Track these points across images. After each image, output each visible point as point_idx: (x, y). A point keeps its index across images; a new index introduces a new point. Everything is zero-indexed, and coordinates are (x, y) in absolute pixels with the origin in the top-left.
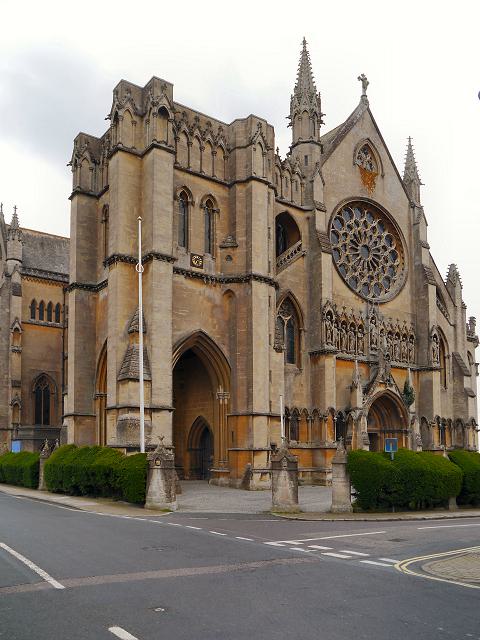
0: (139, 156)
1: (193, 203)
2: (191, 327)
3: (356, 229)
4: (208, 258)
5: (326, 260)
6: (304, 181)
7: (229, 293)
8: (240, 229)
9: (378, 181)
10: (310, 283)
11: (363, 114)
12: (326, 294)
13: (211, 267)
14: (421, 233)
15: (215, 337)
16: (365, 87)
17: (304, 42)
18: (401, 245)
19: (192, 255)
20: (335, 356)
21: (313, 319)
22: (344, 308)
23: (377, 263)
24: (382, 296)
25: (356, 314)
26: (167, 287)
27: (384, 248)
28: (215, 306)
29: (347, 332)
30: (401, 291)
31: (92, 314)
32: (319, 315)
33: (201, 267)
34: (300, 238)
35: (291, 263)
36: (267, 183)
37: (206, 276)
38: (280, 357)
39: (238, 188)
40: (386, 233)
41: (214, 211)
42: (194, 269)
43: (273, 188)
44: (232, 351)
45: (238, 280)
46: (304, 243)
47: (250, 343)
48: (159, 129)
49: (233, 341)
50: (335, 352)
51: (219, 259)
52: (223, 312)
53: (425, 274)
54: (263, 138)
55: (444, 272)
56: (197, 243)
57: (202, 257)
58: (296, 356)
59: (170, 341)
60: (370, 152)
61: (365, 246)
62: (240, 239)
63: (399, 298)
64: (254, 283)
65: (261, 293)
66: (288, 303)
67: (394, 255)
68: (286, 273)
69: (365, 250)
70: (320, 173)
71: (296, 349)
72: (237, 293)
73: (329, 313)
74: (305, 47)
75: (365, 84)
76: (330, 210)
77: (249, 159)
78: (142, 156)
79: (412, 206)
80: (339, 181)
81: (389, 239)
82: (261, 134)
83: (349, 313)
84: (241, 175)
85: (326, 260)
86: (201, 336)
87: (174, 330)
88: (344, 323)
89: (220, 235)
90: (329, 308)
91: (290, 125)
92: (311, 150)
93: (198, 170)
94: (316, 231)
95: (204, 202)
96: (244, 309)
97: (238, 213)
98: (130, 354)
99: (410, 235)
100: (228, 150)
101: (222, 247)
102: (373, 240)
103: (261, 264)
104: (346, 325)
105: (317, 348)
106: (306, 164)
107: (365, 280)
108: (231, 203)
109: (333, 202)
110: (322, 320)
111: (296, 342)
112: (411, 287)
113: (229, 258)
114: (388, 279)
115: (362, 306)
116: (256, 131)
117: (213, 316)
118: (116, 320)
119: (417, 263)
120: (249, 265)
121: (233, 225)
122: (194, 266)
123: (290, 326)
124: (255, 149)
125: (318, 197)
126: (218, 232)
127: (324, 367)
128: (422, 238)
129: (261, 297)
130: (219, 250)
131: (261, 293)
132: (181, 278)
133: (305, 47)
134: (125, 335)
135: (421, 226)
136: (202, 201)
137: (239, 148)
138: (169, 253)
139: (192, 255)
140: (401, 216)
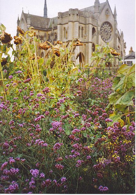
8: (87, 33)
9: (109, 17)
18: (112, 29)
34: (95, 32)
39: (87, 25)
44: (85, 55)
45: (86, 42)
46: (96, 33)
47: (88, 54)
49: (85, 53)
60: (108, 10)
67: (111, 31)
77: (89, 20)
79: (115, 20)
80: (102, 18)
84: (87, 23)
85: (100, 36)
89: (84, 34)
108: (86, 27)
109: (101, 23)
120: (88, 40)
121: (86, 32)
125: (99, 24)
131: (90, 45)
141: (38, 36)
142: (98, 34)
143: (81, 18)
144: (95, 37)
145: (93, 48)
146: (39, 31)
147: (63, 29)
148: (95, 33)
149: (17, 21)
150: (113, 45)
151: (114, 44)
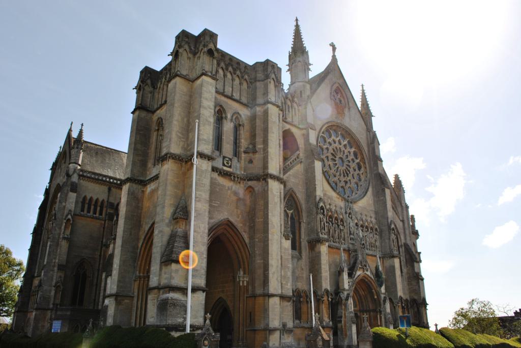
0: (188, 80)
1: (226, 118)
2: (221, 216)
3: (334, 145)
4: (235, 160)
5: (318, 165)
6: (300, 108)
7: (250, 189)
8: (259, 139)
9: (346, 111)
10: (307, 183)
11: (333, 69)
12: (319, 193)
13: (237, 168)
14: (376, 150)
15: (239, 226)
16: (334, 49)
17: (297, 20)
18: (363, 158)
19: (224, 157)
20: (327, 244)
21: (309, 213)
22: (330, 205)
23: (349, 171)
24: (354, 196)
25: (338, 209)
26: (207, 182)
27: (353, 160)
28: (239, 200)
29: (332, 224)
30: (366, 193)
31: (140, 205)
32: (315, 210)
33: (230, 167)
34: (298, 149)
35: (293, 167)
36: (278, 106)
37: (234, 174)
38: (287, 244)
40: (353, 150)
41: (240, 125)
42: (225, 168)
43: (282, 110)
44: (252, 238)
45: (257, 178)
47: (266, 231)
48: (205, 62)
49: (252, 228)
50: (327, 241)
51: (243, 162)
52: (245, 205)
53: (381, 179)
54: (275, 75)
55: (392, 180)
56: (228, 149)
57: (231, 160)
58: (297, 244)
59: (207, 226)
61: (341, 158)
62: (259, 146)
63: (365, 198)
64: (270, 181)
65: (275, 188)
66: (290, 200)
68: (289, 175)
69: (340, 161)
70: (310, 102)
71: (297, 238)
72: (256, 189)
73: (322, 208)
74: (297, 23)
75: (333, 47)
76: (318, 128)
78: (193, 81)
81: (355, 154)
82: (274, 72)
83: (333, 208)
85: (318, 165)
86: (229, 224)
87: (210, 218)
88: (331, 217)
89: (244, 143)
90: (321, 204)
91: (289, 70)
92: (304, 86)
93: (230, 95)
94: (310, 144)
95: (234, 117)
96: (262, 202)
97: (257, 128)
98: (173, 237)
99: (369, 151)
100: (251, 82)
101: (245, 152)
102: (346, 154)
103: (274, 166)
104: (334, 220)
105: (313, 236)
106: (301, 96)
107: (343, 184)
110: (317, 213)
111: (297, 231)
112: (373, 191)
113: (251, 161)
114: (357, 184)
115: (342, 204)
116: (268, 68)
117: (237, 208)
118: (164, 207)
119: (375, 172)
120: (265, 166)
121: (253, 136)
122: (224, 165)
123: (292, 218)
124: (270, 82)
126: (243, 141)
127: (320, 252)
128: (377, 154)
129: (275, 193)
130: (243, 155)
132: (215, 175)
133: (297, 23)
134: (170, 222)
135: (376, 143)
136: (232, 117)
137: (259, 81)
138: (209, 154)
139: (224, 157)
140: (362, 138)
141: (105, 204)
142: (307, 157)
143: (233, 80)
144: (299, 168)
145: (290, 212)
146: (110, 189)
147: (154, 126)
148: (298, 152)
149: (51, 165)
150: (373, 216)
151: (376, 213)
